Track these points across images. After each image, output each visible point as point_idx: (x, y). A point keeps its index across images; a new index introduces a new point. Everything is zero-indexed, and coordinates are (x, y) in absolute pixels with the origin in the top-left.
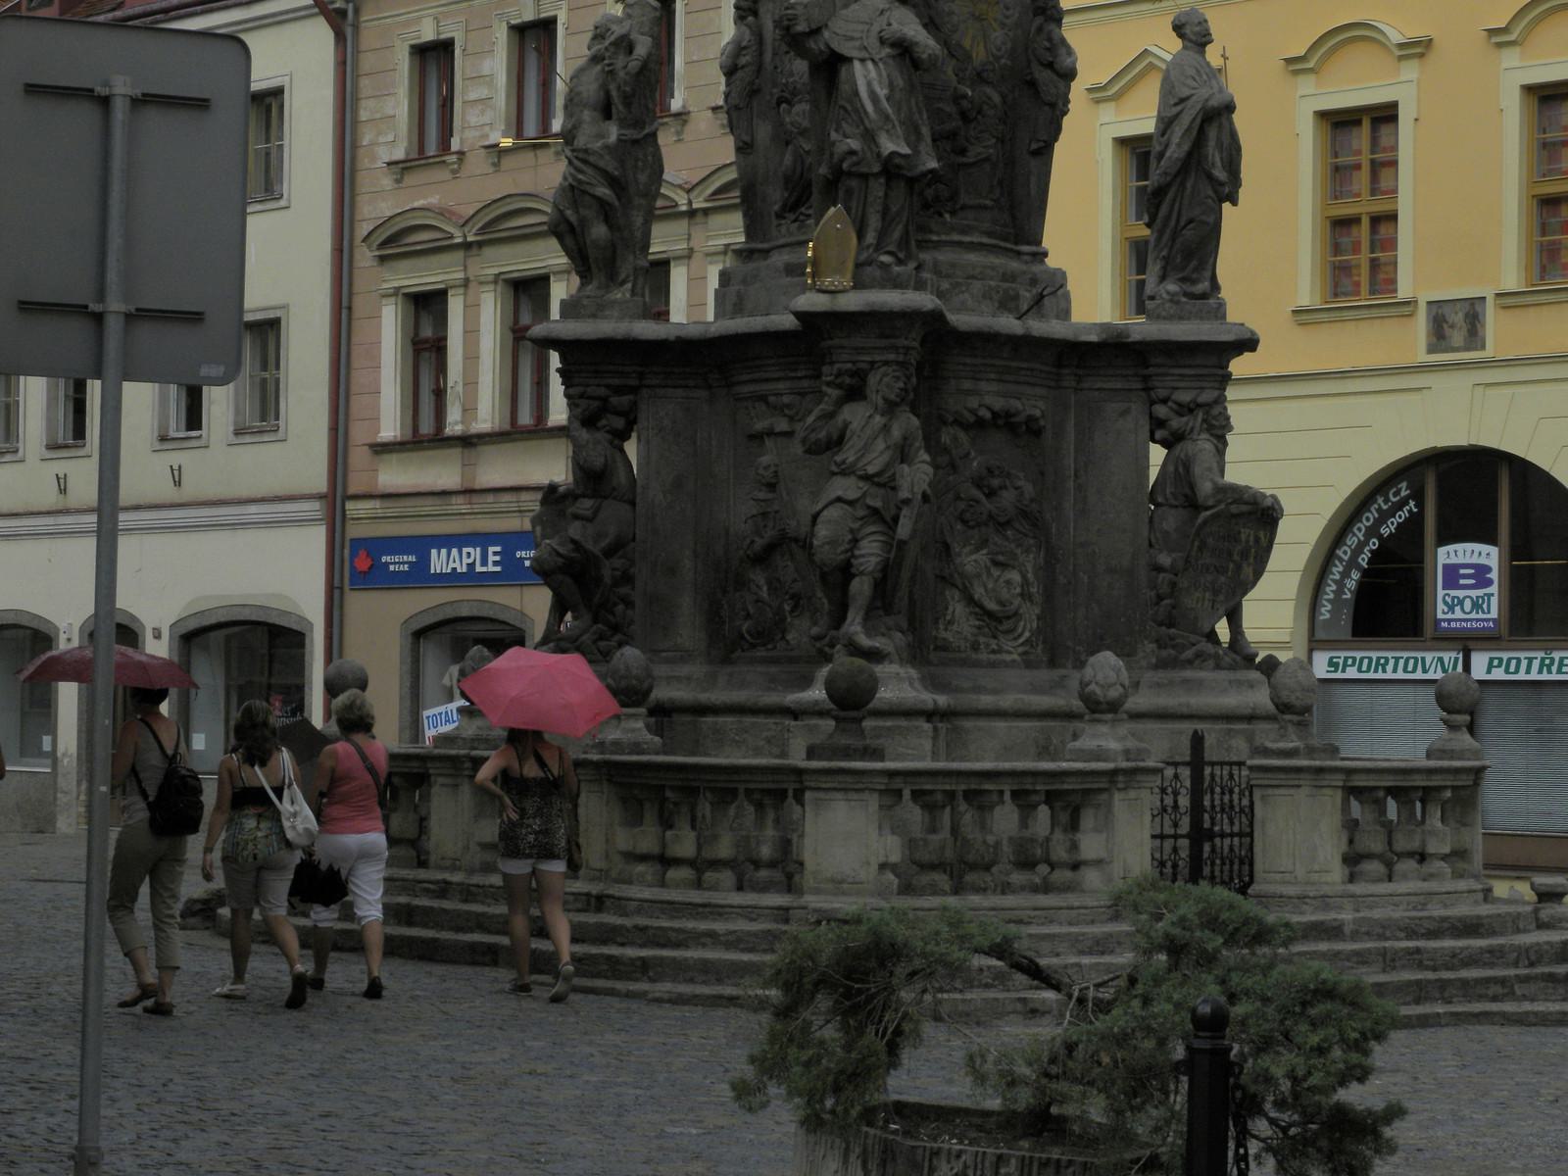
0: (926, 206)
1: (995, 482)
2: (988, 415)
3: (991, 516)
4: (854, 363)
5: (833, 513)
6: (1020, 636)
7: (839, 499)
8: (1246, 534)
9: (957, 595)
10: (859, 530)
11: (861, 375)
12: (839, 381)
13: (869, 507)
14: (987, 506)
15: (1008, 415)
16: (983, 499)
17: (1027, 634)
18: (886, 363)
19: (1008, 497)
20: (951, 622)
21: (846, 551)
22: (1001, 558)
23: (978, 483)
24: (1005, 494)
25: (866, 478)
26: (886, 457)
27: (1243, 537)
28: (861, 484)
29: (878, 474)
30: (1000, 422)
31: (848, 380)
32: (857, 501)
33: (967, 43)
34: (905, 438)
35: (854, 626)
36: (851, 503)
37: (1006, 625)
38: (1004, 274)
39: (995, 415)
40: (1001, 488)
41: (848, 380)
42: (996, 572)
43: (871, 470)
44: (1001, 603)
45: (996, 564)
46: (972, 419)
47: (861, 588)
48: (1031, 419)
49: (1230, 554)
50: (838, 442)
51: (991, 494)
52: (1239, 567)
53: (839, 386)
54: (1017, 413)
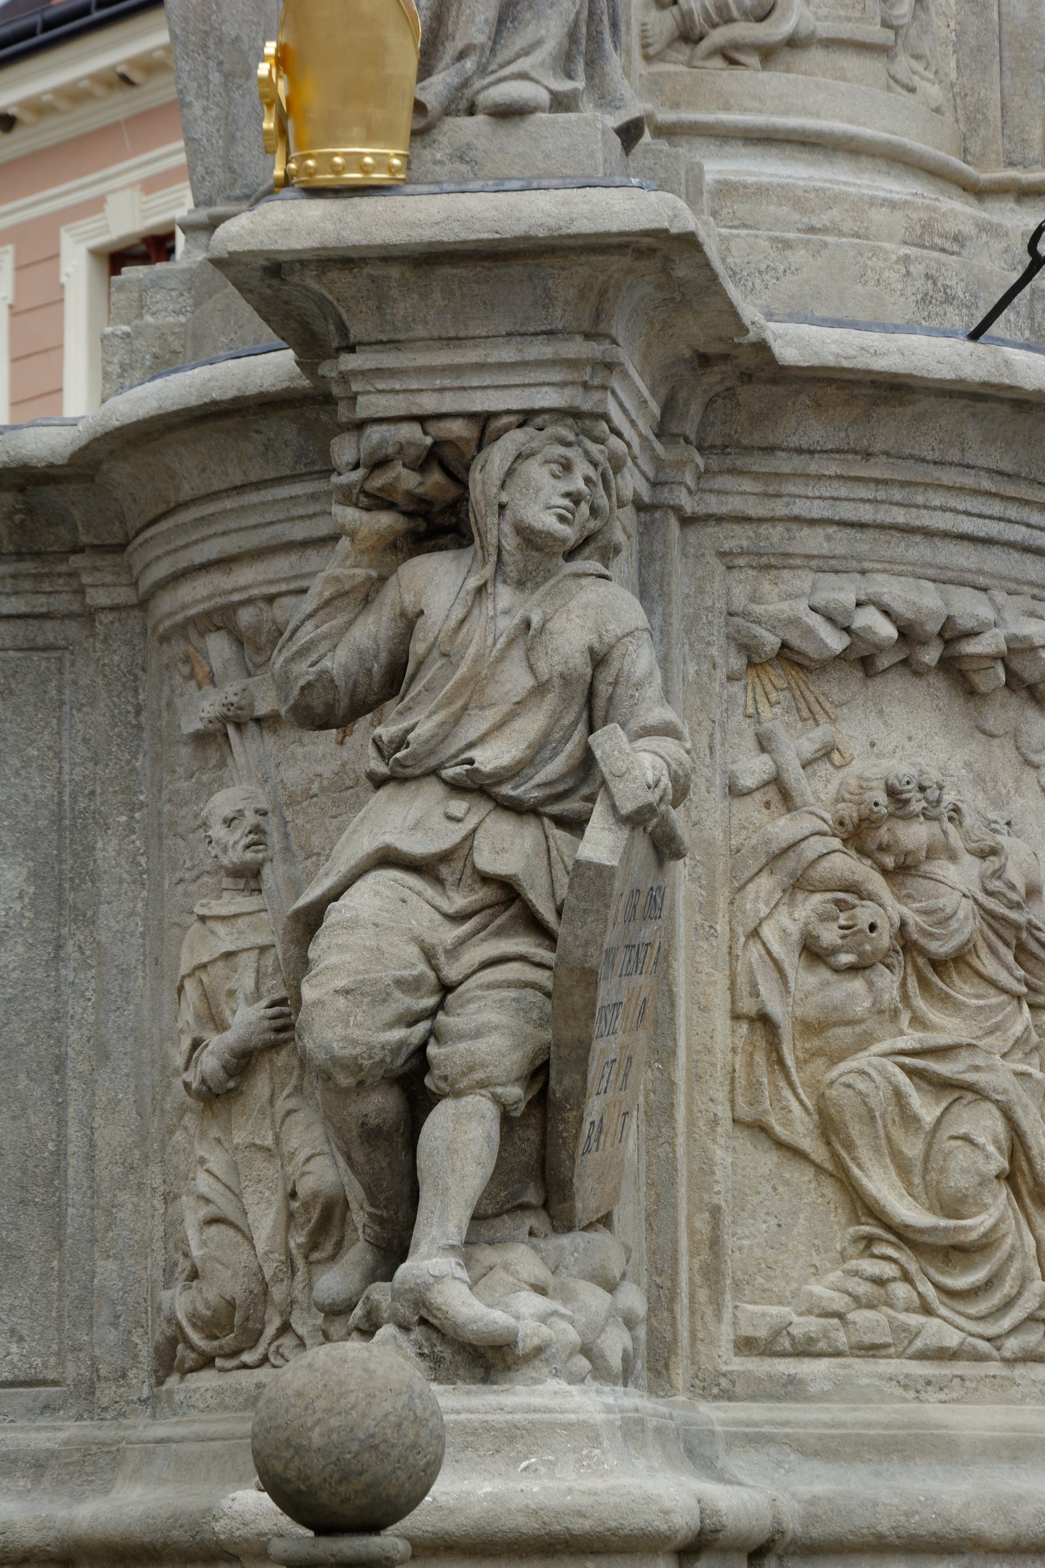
0: (688, 36)
1: (915, 835)
2: (887, 630)
3: (906, 943)
4: (422, 420)
5: (373, 897)
6: (1008, 1304)
7: (388, 859)
10: (455, 950)
11: (450, 461)
12: (378, 481)
13: (486, 879)
14: (887, 908)
15: (951, 635)
16: (877, 883)
18: (526, 417)
21: (412, 1020)
22: (944, 1068)
24: (943, 869)
25: (476, 787)
26: (530, 726)
28: (458, 806)
29: (504, 775)
30: (931, 655)
31: (409, 480)
32: (445, 857)
34: (598, 660)
35: (431, 1260)
36: (421, 867)
38: (927, 227)
39: (907, 634)
40: (931, 854)
41: (409, 480)
43: (490, 758)
46: (836, 642)
47: (460, 1145)
50: (393, 678)
51: (902, 870)
53: (378, 502)
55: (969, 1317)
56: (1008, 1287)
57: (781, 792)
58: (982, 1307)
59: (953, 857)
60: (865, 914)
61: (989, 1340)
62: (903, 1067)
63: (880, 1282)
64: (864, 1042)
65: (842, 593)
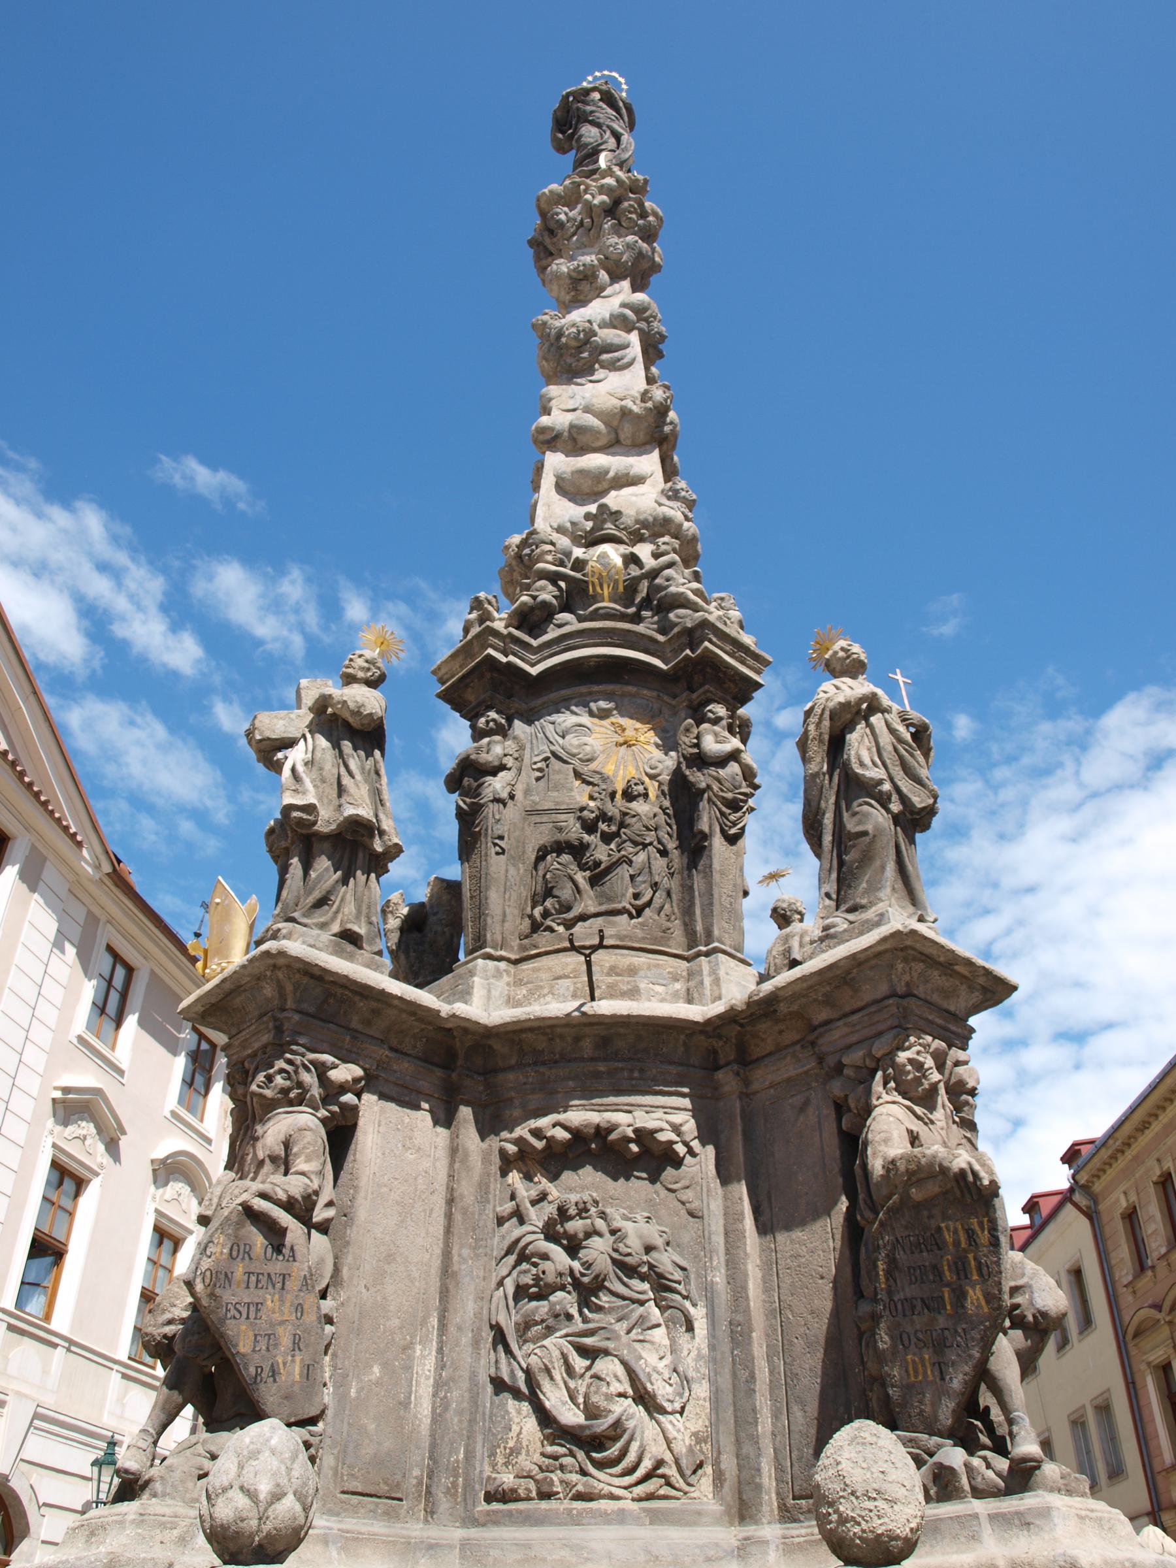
0: (536, 927)
1: (575, 1226)
8: (951, 1231)
9: (525, 1406)
15: (601, 1132)
17: (647, 1465)
19: (598, 1250)
20: (515, 1451)
22: (588, 1341)
23: (550, 1233)
24: (595, 1241)
27: (948, 1237)
33: (609, 769)
37: (614, 1451)
40: (588, 1235)
42: (579, 1363)
44: (592, 1412)
45: (583, 1351)
46: (539, 1145)
48: (643, 1136)
49: (936, 1269)
52: (960, 1296)
54: (613, 1128)
55: (611, 1475)
56: (631, 1457)
57: (519, 1216)
58: (618, 1469)
59: (600, 1235)
60: (546, 1265)
61: (626, 1488)
62: (569, 1342)
63: (555, 1458)
64: (550, 1331)
65: (543, 1122)
